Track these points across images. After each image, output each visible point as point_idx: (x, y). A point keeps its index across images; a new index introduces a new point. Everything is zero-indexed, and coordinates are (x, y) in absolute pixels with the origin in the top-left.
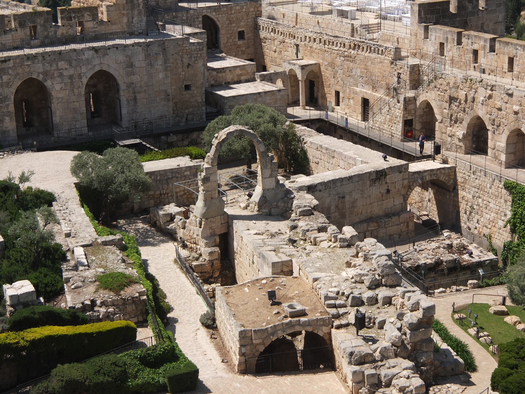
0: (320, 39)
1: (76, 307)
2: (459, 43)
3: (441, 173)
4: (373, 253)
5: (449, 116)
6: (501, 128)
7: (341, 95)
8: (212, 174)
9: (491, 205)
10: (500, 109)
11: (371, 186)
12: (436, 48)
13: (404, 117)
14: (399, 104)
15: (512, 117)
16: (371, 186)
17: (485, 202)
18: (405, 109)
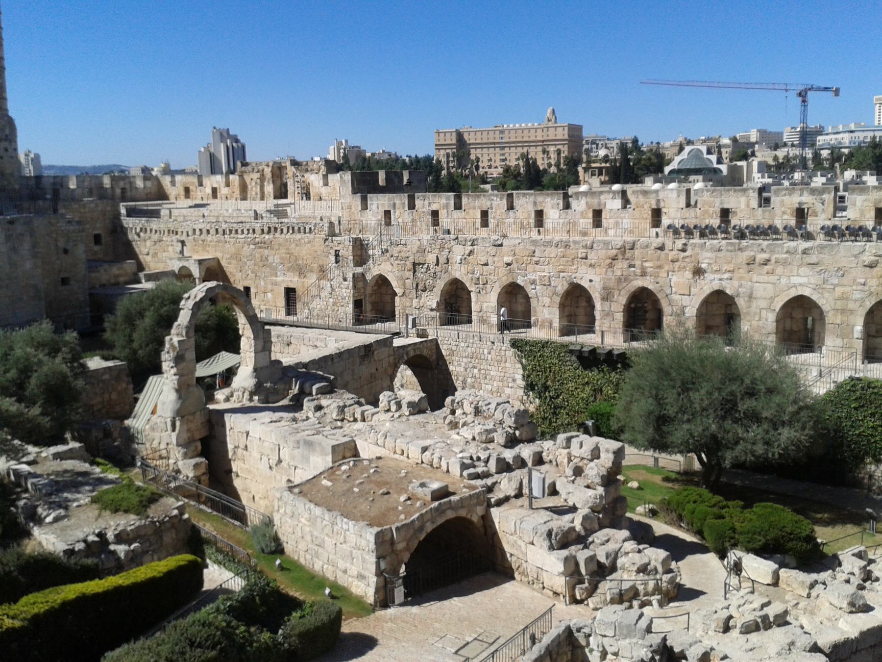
0: (217, 230)
1: (76, 549)
2: (412, 206)
3: (423, 346)
4: (486, 402)
5: (415, 286)
6: (488, 286)
7: (253, 291)
8: (187, 349)
9: (492, 373)
10: (486, 264)
11: (360, 364)
12: (379, 217)
13: (354, 297)
14: (346, 283)
15: (503, 271)
16: (360, 364)
17: (483, 372)
18: (355, 287)
